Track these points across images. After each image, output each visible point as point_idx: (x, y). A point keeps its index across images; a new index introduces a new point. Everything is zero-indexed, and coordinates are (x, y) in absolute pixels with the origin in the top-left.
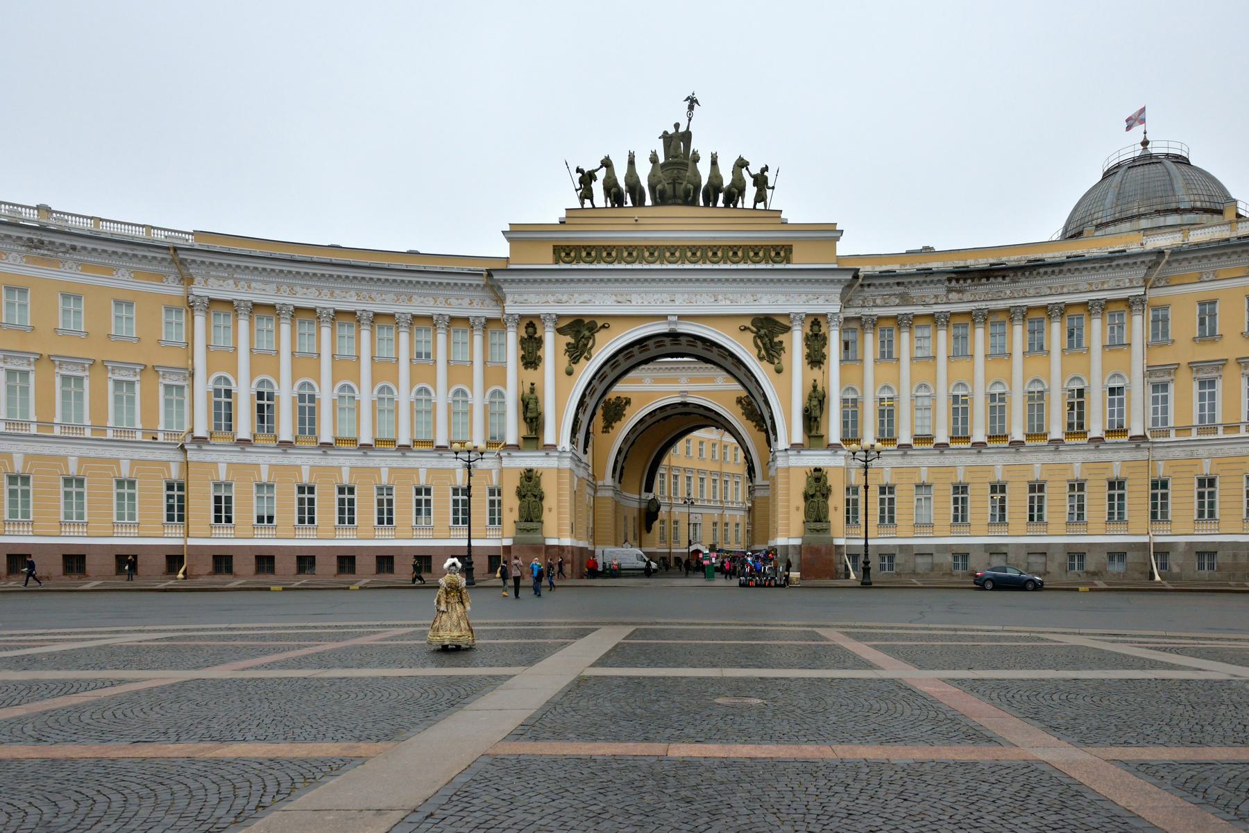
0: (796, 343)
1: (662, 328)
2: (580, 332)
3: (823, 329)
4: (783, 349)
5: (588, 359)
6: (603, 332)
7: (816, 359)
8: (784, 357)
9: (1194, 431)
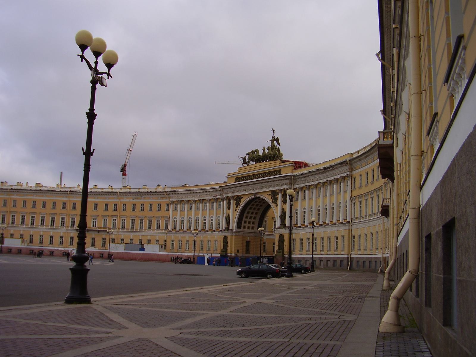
0: (280, 197)
1: (253, 197)
2: (238, 199)
7: (284, 202)
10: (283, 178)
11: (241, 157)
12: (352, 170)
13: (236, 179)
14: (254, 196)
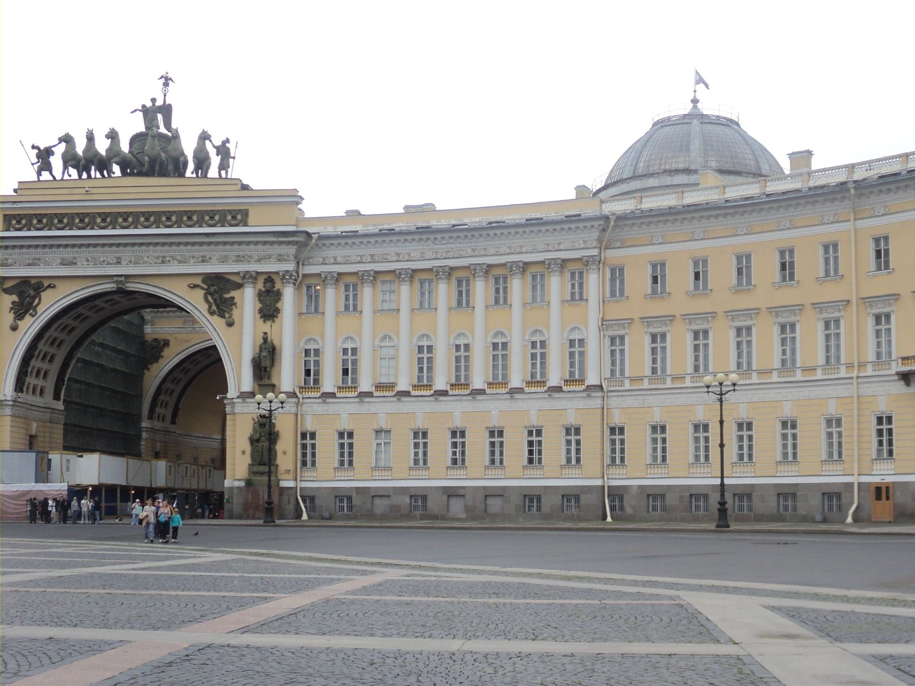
0: (247, 300)
1: (109, 286)
3: (278, 286)
4: (235, 304)
5: (33, 316)
6: (49, 291)
8: (235, 312)
9: (646, 381)
10: (275, 239)
11: (33, 147)
12: (604, 244)
13: (7, 218)
14: (114, 285)
